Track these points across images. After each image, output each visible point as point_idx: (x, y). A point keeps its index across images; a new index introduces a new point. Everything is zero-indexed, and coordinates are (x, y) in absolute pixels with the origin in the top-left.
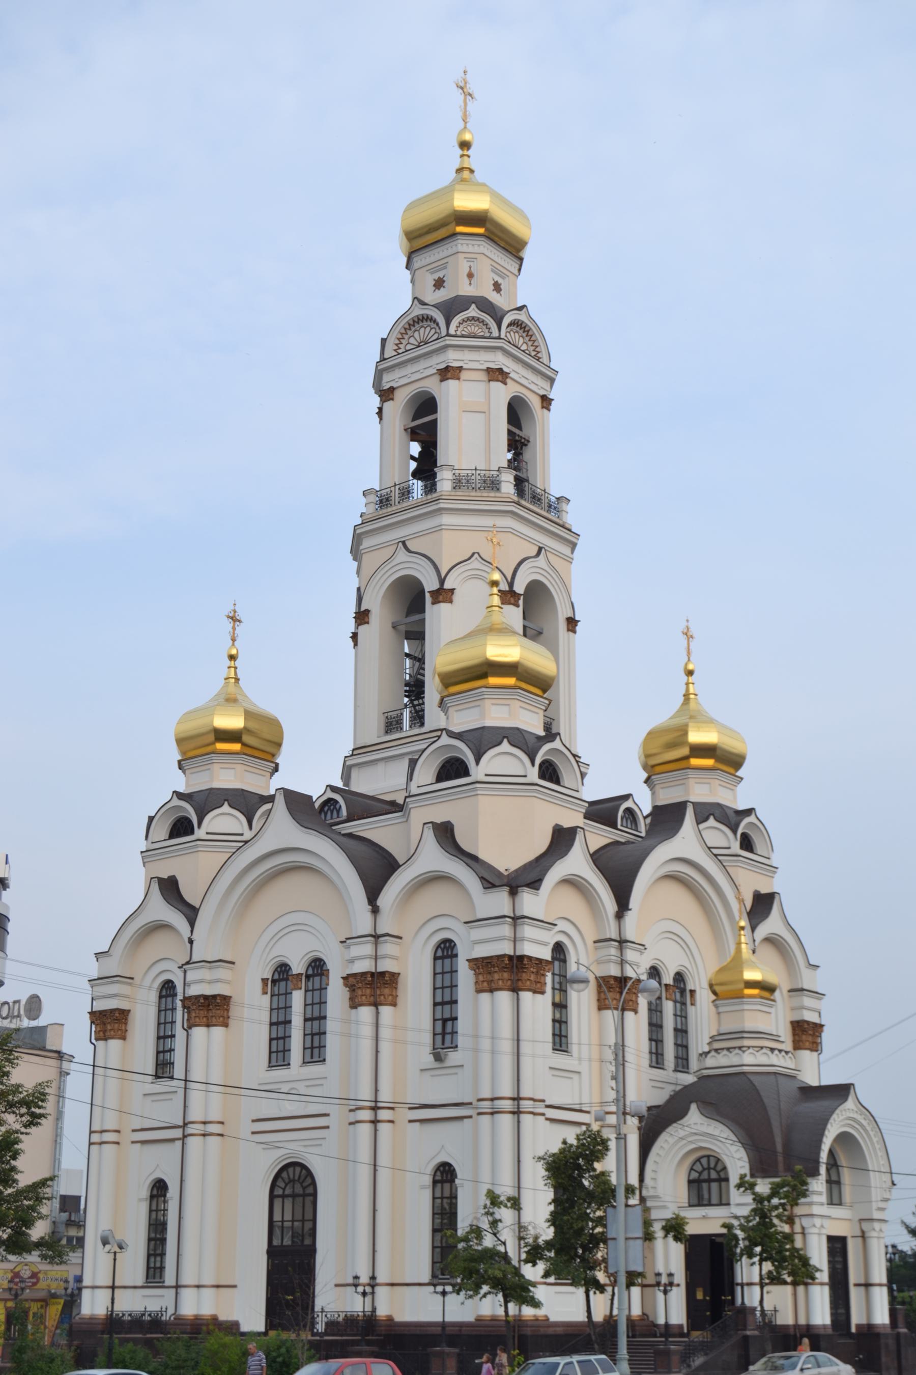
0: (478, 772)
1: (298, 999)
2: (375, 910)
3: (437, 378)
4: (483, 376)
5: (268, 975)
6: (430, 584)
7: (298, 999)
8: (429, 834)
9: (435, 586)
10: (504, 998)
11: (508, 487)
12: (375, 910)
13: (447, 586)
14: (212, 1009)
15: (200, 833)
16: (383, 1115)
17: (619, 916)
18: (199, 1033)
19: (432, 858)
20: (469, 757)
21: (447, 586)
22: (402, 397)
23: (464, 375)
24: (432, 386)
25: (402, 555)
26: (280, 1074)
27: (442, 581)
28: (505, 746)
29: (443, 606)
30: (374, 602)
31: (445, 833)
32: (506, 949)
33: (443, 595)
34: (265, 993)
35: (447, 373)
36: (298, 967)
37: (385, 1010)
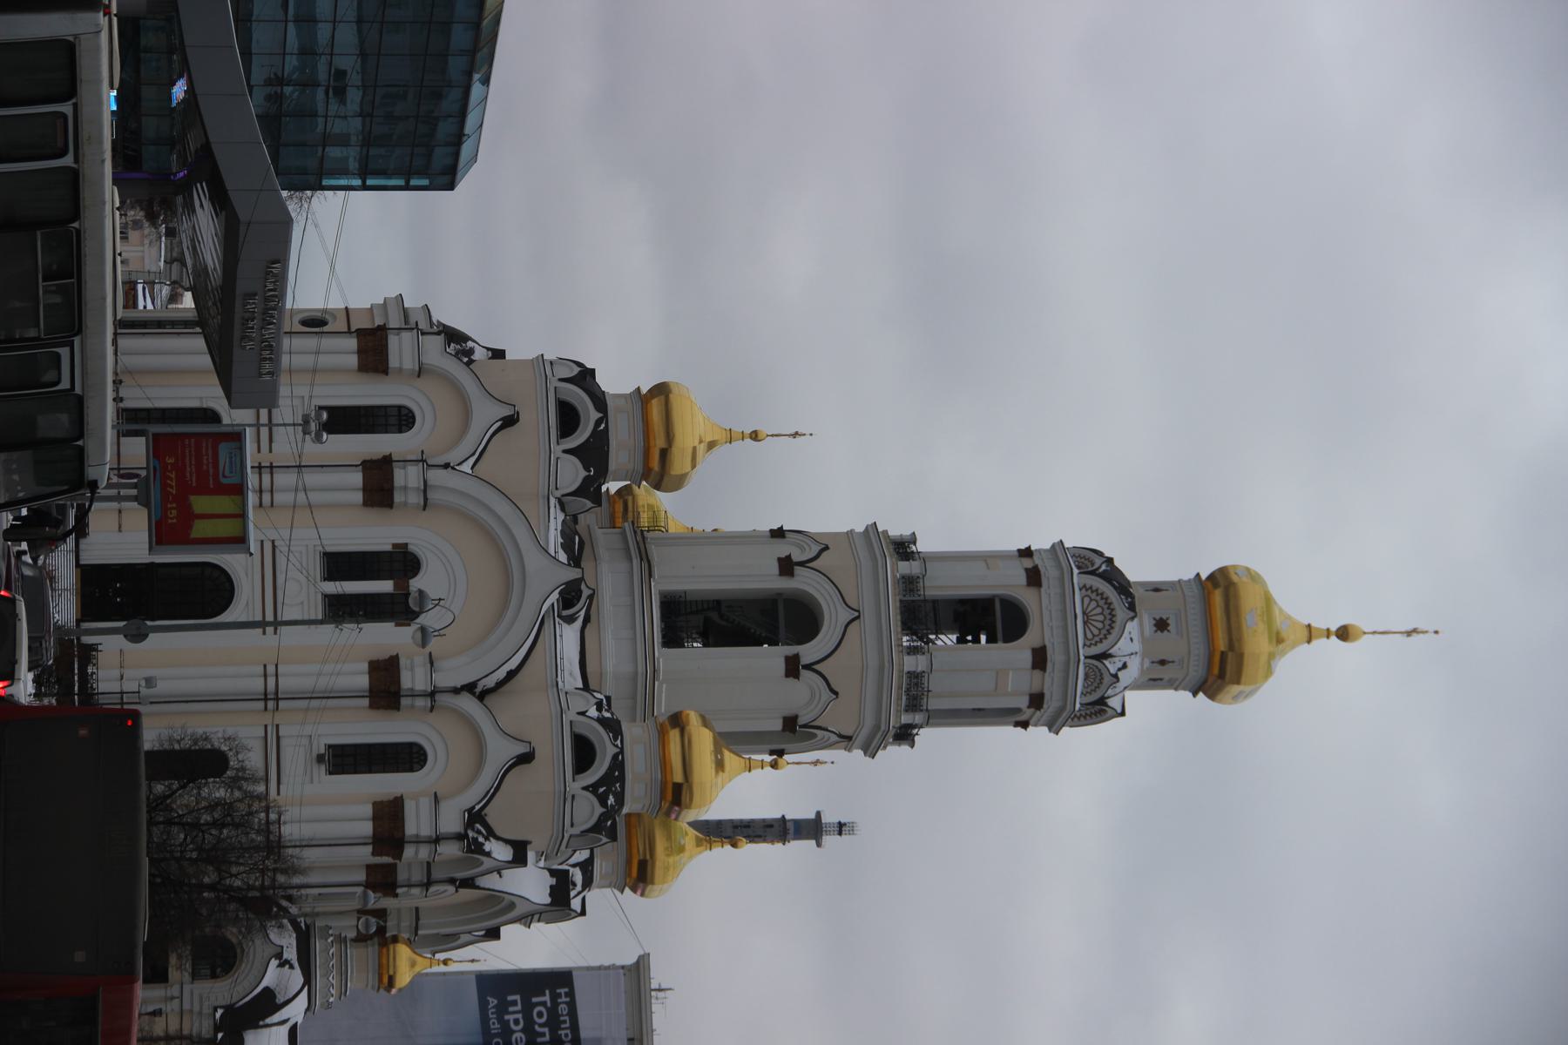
0: (576, 786)
1: (385, 586)
2: (456, 691)
3: (1037, 644)
4: (1036, 689)
5: (411, 548)
6: (809, 652)
7: (385, 586)
8: (521, 749)
9: (805, 660)
10: (367, 828)
11: (906, 719)
12: (456, 691)
13: (804, 673)
14: (378, 485)
15: (557, 450)
16: (271, 704)
17: (452, 881)
18: (357, 478)
19: (501, 751)
20: (592, 776)
21: (804, 673)
22: (1027, 597)
23: (1037, 673)
24: (1030, 639)
25: (845, 615)
26: (316, 568)
27: (808, 667)
28: (599, 810)
29: (781, 666)
30: (804, 581)
31: (526, 758)
32: (410, 829)
33: (793, 668)
34: (395, 546)
35: (1040, 659)
36: (415, 584)
37: (366, 702)
